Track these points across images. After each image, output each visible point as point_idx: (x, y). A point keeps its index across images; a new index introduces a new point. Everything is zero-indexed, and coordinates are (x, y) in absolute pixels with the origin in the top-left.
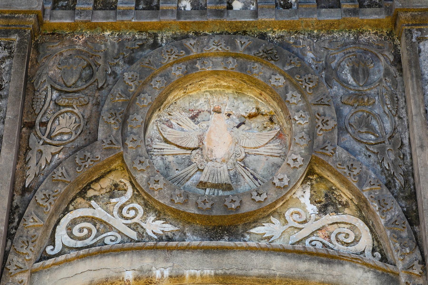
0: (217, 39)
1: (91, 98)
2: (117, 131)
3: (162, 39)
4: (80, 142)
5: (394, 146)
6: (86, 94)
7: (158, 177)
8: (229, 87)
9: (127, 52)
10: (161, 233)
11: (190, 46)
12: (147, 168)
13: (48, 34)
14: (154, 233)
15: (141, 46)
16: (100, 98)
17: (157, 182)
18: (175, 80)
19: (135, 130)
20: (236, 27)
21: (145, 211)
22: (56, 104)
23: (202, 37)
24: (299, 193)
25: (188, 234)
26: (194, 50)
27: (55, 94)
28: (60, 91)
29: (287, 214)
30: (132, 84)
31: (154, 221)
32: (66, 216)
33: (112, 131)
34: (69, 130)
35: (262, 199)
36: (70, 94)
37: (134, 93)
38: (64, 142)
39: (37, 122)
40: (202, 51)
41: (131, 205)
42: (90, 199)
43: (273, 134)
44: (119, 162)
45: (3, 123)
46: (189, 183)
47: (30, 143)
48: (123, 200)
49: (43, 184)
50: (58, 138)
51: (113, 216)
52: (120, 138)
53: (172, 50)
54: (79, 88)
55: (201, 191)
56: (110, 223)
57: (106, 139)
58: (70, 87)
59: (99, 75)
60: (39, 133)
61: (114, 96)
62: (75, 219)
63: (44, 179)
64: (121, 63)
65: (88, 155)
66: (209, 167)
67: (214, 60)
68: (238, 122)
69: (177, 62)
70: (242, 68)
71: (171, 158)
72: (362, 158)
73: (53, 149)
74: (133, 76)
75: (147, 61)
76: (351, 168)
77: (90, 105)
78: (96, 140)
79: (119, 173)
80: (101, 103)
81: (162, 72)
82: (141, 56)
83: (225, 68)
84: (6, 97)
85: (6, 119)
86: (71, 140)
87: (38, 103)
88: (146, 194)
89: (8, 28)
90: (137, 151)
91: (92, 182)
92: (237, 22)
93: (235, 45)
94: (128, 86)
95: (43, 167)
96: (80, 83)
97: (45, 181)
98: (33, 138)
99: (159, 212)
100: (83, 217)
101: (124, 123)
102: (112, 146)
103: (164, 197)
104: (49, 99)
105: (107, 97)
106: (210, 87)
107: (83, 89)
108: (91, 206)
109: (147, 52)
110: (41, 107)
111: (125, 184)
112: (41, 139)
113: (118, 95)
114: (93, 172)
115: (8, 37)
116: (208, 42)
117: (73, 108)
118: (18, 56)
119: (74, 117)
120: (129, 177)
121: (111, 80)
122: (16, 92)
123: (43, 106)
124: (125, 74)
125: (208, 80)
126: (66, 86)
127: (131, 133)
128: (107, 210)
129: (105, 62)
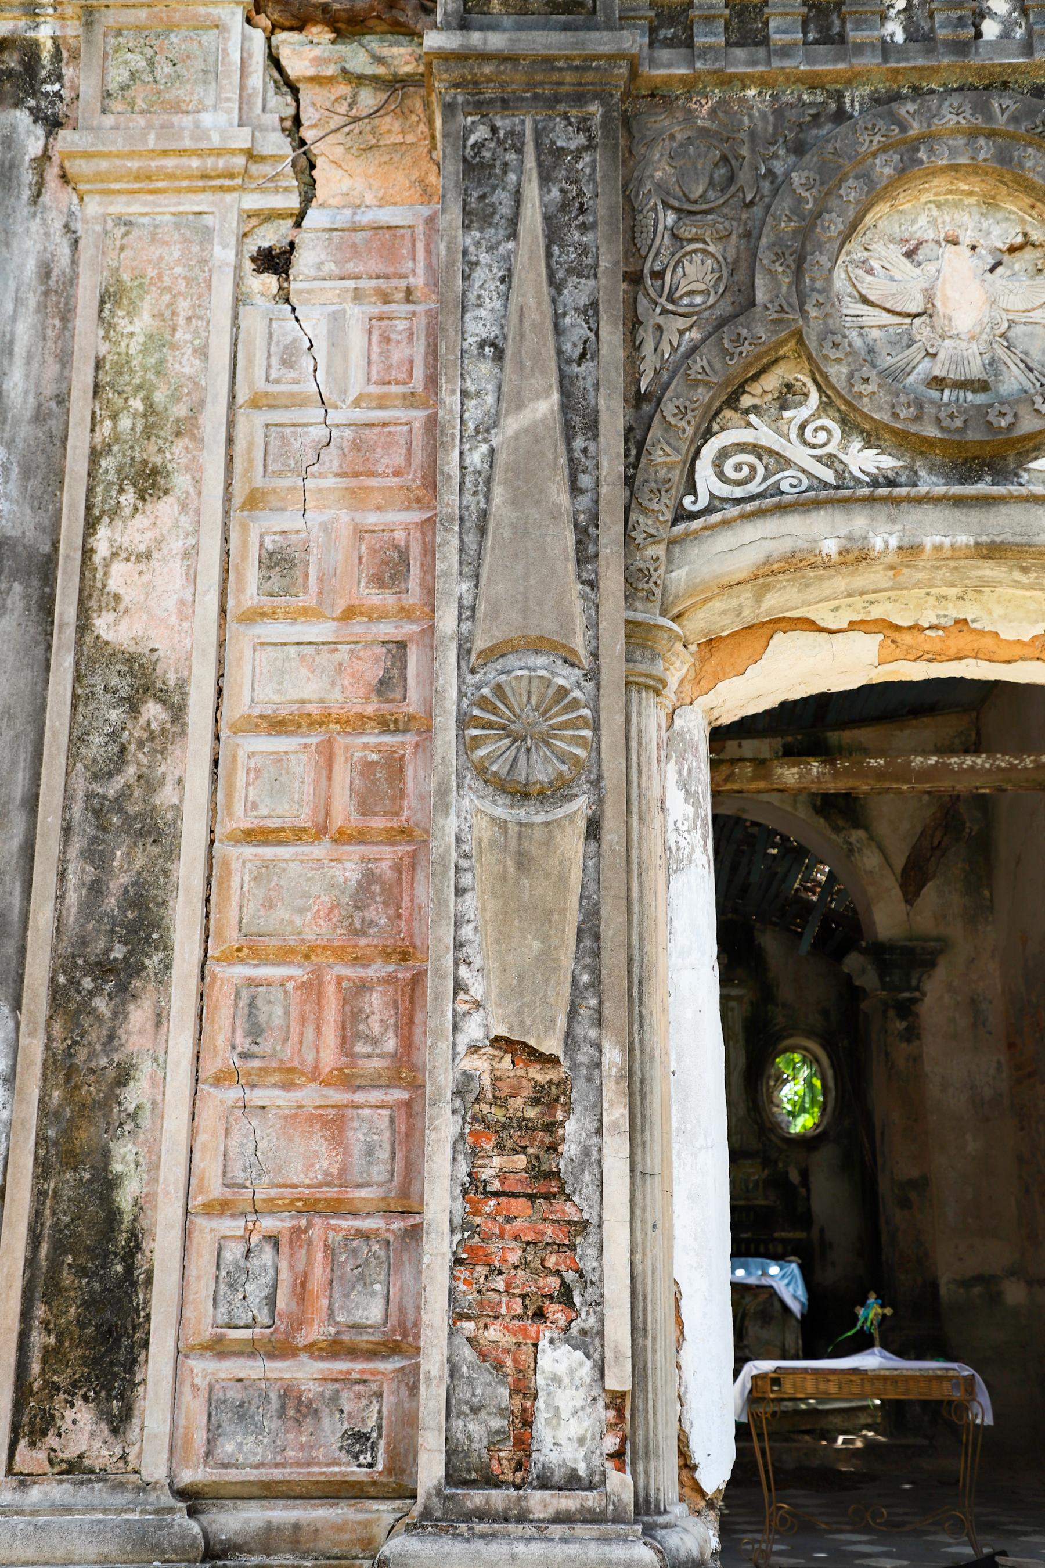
0: (955, 100)
1: (735, 224)
2: (789, 287)
3: (852, 102)
4: (725, 308)
6: (725, 216)
7: (866, 372)
8: (971, 194)
9: (791, 130)
10: (876, 471)
11: (907, 116)
12: (847, 354)
13: (644, 97)
14: (863, 472)
15: (815, 117)
16: (750, 223)
17: (866, 381)
18: (883, 184)
19: (818, 285)
20: (991, 74)
21: (843, 432)
22: (674, 236)
23: (927, 97)
25: (922, 473)
26: (915, 125)
27: (671, 218)
28: (678, 210)
30: (807, 194)
31: (860, 450)
32: (709, 442)
33: (780, 287)
34: (703, 287)
36: (699, 217)
37: (811, 211)
38: (697, 309)
39: (646, 271)
40: (929, 125)
41: (819, 423)
42: (747, 412)
44: (792, 344)
45: (596, 276)
46: (911, 379)
47: (639, 311)
48: (803, 413)
49: (672, 387)
50: (686, 301)
51: (789, 441)
52: (794, 299)
53: (874, 125)
54: (712, 205)
55: (935, 394)
56: (787, 454)
57: (772, 302)
58: (696, 202)
59: (744, 176)
60: (651, 292)
61: (777, 219)
62: (724, 448)
63: (671, 379)
64: (781, 152)
65: (744, 332)
67: (950, 142)
69: (884, 149)
70: (1004, 158)
73: (681, 323)
74: (808, 178)
75: (830, 147)
77: (734, 237)
78: (753, 304)
79: (792, 364)
80: (755, 233)
81: (858, 170)
82: (816, 137)
83: (973, 158)
84: (593, 226)
85: (601, 270)
86: (709, 304)
87: (644, 235)
88: (847, 402)
89: (581, 89)
90: (825, 323)
91: (746, 381)
92: (993, 65)
93: (989, 110)
94: (800, 200)
95: (667, 356)
96: (711, 195)
97: (675, 382)
98: (643, 302)
99: (869, 435)
100: (738, 444)
101: (799, 272)
102: (783, 315)
103: (880, 409)
104: (661, 227)
105: (763, 223)
106: (936, 194)
107: (719, 207)
108: (749, 424)
110: (649, 242)
111: (804, 384)
112: (656, 304)
113: (784, 218)
114: (751, 364)
115: (581, 107)
116: (940, 107)
117: (705, 243)
118: (605, 145)
119: (709, 262)
120: (812, 373)
121: (766, 186)
122: (611, 216)
123: (653, 240)
124: (793, 175)
125: (936, 182)
126: (688, 200)
127: (812, 290)
128: (777, 431)
129: (753, 151)
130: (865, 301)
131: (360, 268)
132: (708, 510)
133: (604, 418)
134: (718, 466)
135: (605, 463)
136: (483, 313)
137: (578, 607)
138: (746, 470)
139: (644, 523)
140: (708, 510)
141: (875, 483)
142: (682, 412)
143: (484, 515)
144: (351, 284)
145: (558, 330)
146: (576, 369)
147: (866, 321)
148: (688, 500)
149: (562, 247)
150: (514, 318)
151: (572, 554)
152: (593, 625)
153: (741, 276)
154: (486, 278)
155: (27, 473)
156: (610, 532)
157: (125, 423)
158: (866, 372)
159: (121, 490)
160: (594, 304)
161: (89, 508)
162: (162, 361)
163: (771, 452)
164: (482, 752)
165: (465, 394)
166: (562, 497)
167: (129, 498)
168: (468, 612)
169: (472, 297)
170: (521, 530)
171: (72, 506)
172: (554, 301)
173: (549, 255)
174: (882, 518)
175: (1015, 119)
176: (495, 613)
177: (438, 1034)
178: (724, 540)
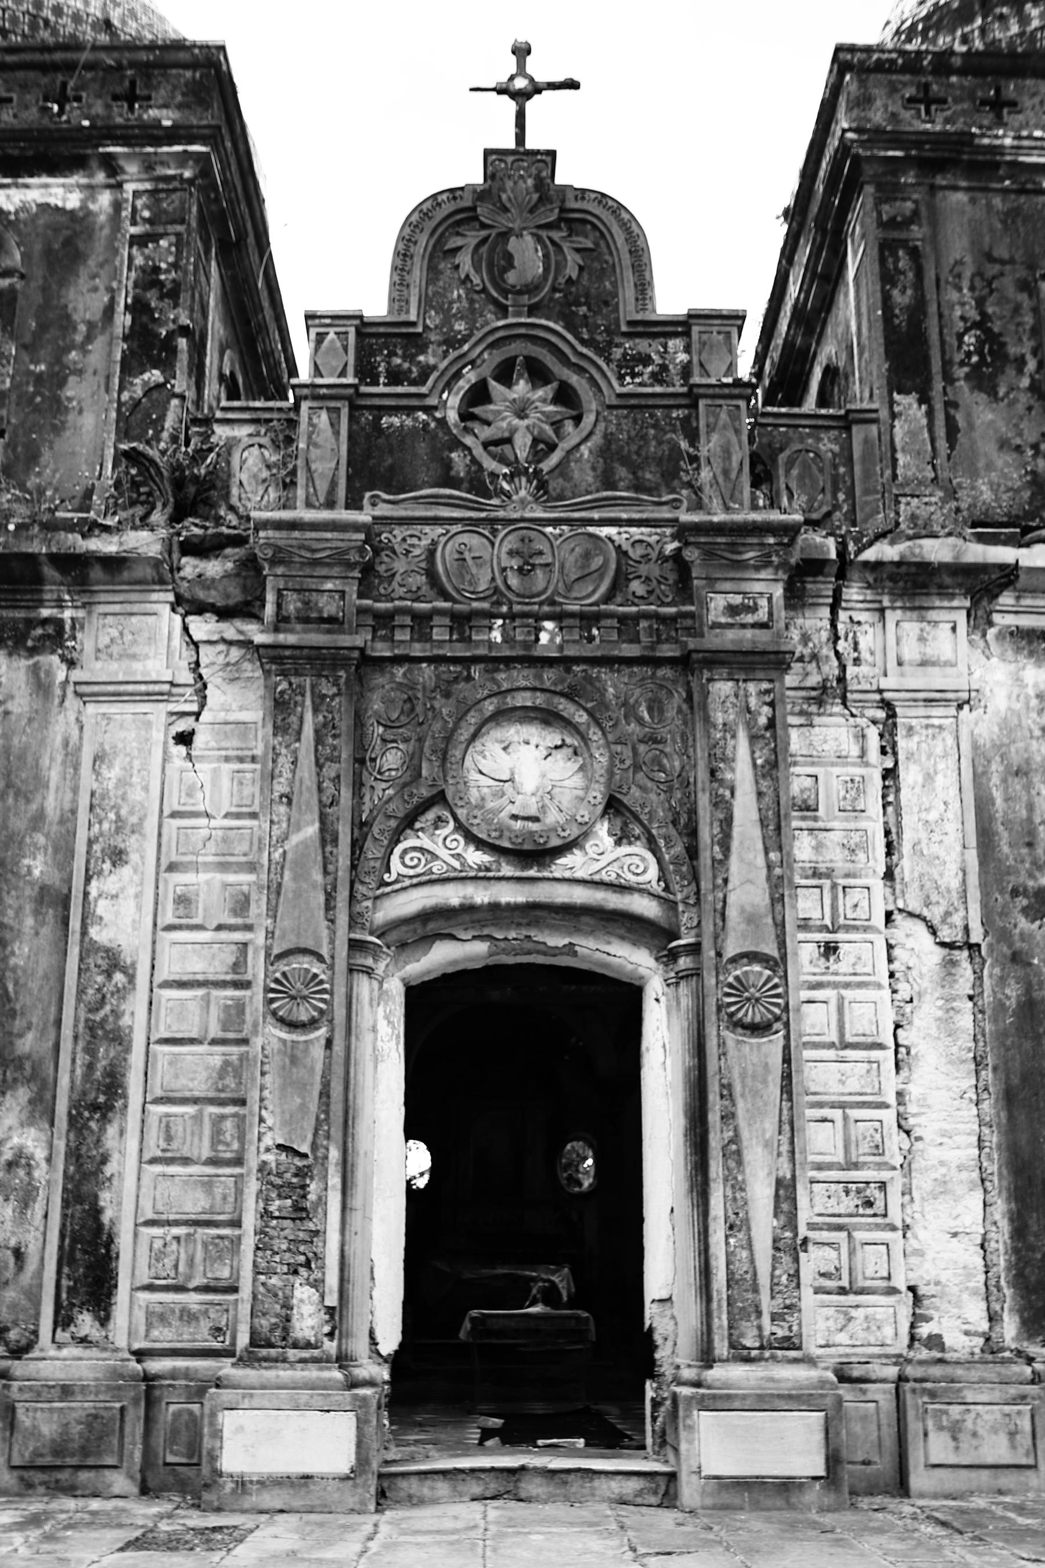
4: (407, 778)
5: (681, 784)
24: (598, 826)
29: (587, 846)
35: (565, 834)
43: (577, 766)
46: (502, 814)
55: (512, 822)
66: (519, 799)
68: (545, 753)
69: (490, 696)
71: (485, 790)
72: (653, 796)
73: (384, 785)
76: (643, 806)
96: (402, 718)
98: (365, 773)
101: (444, 759)
109: (462, 685)
130: (481, 773)
131: (228, 745)
132: (396, 881)
133: (341, 836)
134: (402, 857)
135: (341, 860)
136: (282, 780)
137: (325, 933)
138: (416, 861)
139: (361, 888)
140: (396, 881)
141: (480, 869)
142: (382, 832)
143: (280, 885)
144: (224, 753)
145: (320, 790)
146: (328, 810)
147: (481, 783)
148: (386, 876)
149: (323, 745)
150: (297, 783)
151: (323, 906)
152: (332, 942)
153: (415, 761)
154: (284, 762)
155: (56, 850)
156: (342, 896)
157: (106, 826)
158: (476, 812)
159: (104, 861)
160: (338, 777)
161: (87, 870)
162: (125, 793)
163: (429, 852)
164: (275, 1005)
165: (272, 822)
166: (318, 877)
167: (107, 866)
168: (270, 934)
169: (277, 771)
170: (298, 894)
171: (79, 869)
172: (318, 775)
173: (316, 750)
174: (481, 888)
175: (555, 684)
176: (283, 936)
177: (251, 1143)
178: (402, 897)
